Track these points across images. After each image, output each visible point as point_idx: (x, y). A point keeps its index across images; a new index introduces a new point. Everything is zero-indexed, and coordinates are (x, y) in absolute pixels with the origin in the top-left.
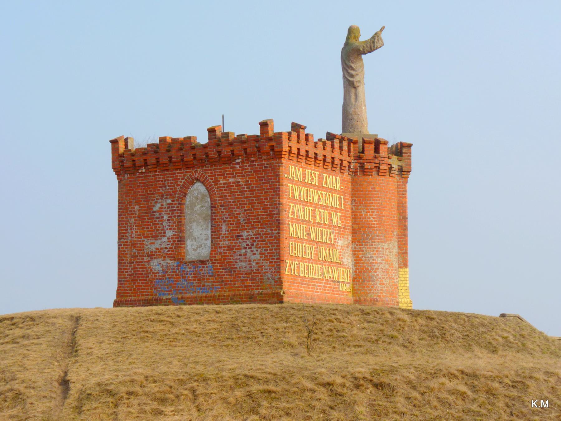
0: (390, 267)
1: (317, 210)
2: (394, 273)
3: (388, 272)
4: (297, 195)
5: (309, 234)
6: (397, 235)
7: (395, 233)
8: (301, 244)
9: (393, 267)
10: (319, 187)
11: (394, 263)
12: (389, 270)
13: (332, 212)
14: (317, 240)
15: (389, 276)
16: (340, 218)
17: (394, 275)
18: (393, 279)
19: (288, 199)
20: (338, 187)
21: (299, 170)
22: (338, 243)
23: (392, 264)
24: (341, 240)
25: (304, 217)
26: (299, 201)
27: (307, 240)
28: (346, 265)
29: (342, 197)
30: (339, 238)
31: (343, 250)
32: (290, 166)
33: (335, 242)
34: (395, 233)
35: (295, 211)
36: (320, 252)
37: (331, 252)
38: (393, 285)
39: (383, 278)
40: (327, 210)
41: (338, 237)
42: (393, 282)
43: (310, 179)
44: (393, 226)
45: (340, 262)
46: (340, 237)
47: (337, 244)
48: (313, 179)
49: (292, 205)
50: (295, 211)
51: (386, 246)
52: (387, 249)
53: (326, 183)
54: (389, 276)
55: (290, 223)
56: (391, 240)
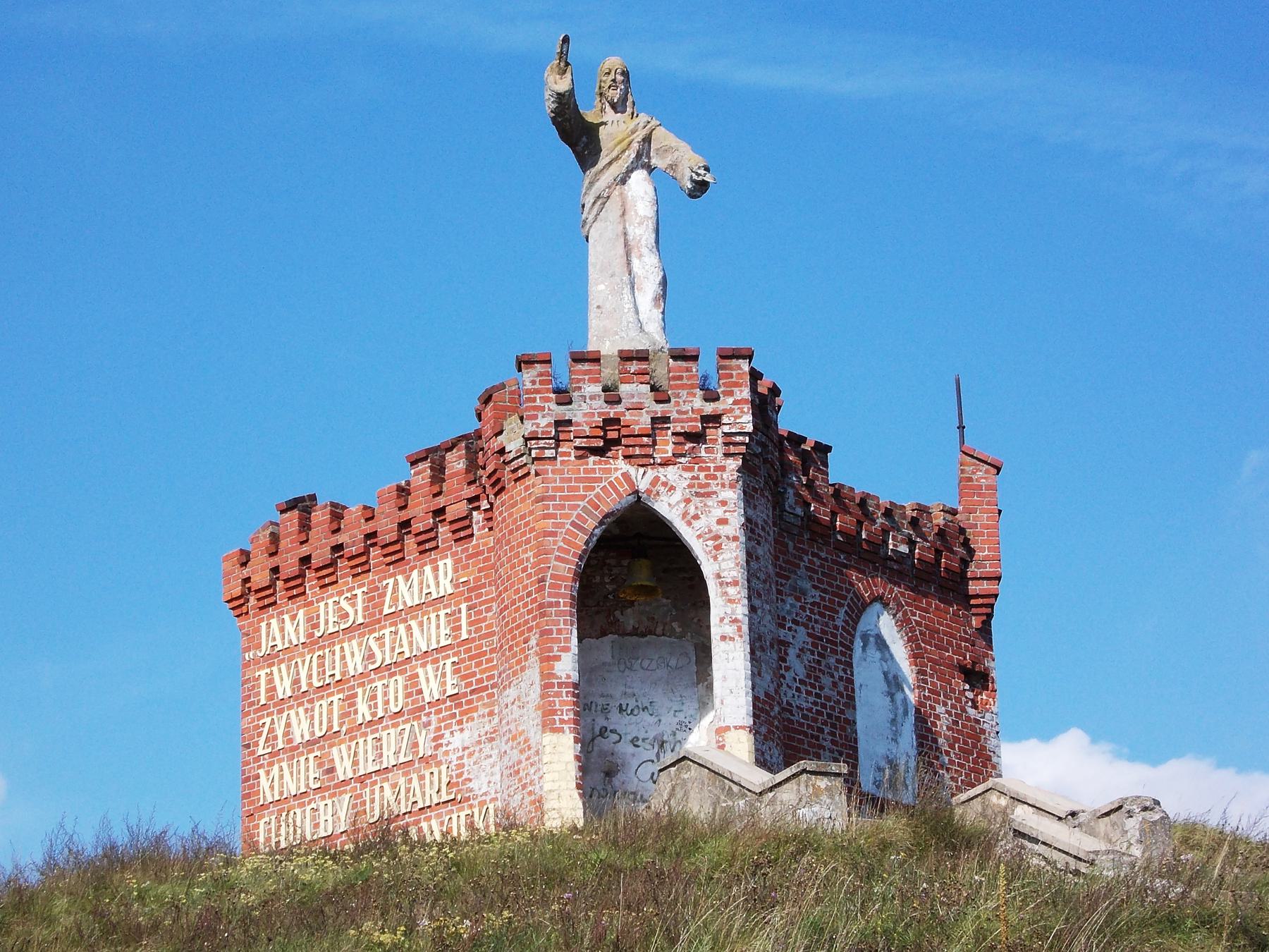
0: (522, 752)
1: (360, 691)
2: (532, 765)
3: (518, 772)
4: (284, 688)
5: (332, 770)
6: (537, 645)
7: (533, 642)
8: (298, 811)
9: (529, 747)
10: (373, 622)
11: (532, 734)
12: (519, 762)
13: (420, 671)
14: (362, 772)
15: (520, 780)
16: (456, 671)
17: (532, 771)
18: (532, 782)
19: (256, 711)
20: (446, 587)
21: (293, 617)
22: (449, 743)
23: (526, 741)
24: (462, 730)
25: (313, 733)
26: (297, 698)
27: (328, 788)
28: (485, 794)
29: (464, 606)
30: (455, 727)
31: (470, 755)
32: (263, 625)
33: (437, 747)
34: (533, 642)
35: (280, 732)
36: (373, 801)
37: (415, 783)
38: (533, 802)
39: (509, 796)
40: (402, 672)
41: (446, 727)
42: (530, 793)
43: (331, 620)
44: (526, 622)
45: (452, 797)
46: (460, 722)
47: (444, 748)
48: (347, 615)
49: (268, 720)
50: (280, 732)
51: (512, 693)
52: (513, 703)
53: (395, 600)
54: (520, 780)
55: (261, 772)
56: (523, 669)
